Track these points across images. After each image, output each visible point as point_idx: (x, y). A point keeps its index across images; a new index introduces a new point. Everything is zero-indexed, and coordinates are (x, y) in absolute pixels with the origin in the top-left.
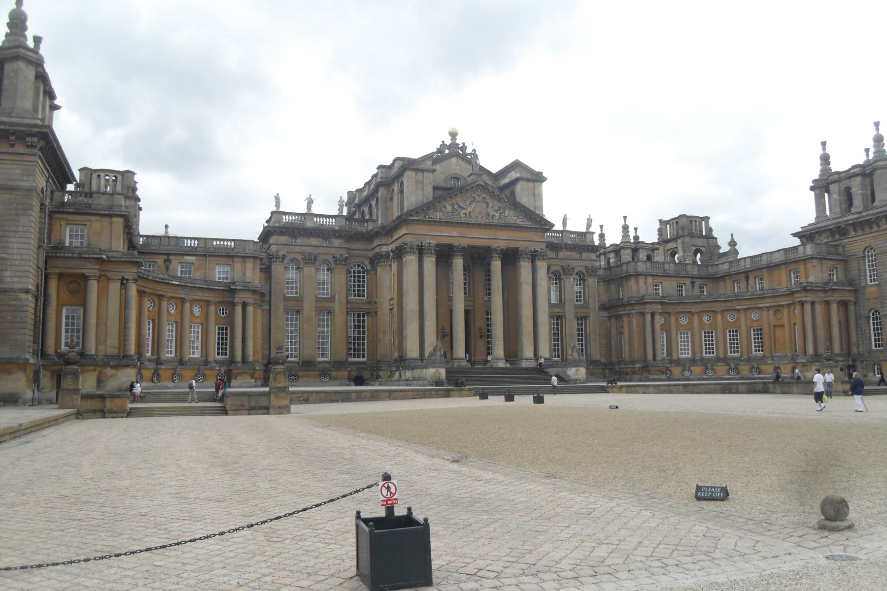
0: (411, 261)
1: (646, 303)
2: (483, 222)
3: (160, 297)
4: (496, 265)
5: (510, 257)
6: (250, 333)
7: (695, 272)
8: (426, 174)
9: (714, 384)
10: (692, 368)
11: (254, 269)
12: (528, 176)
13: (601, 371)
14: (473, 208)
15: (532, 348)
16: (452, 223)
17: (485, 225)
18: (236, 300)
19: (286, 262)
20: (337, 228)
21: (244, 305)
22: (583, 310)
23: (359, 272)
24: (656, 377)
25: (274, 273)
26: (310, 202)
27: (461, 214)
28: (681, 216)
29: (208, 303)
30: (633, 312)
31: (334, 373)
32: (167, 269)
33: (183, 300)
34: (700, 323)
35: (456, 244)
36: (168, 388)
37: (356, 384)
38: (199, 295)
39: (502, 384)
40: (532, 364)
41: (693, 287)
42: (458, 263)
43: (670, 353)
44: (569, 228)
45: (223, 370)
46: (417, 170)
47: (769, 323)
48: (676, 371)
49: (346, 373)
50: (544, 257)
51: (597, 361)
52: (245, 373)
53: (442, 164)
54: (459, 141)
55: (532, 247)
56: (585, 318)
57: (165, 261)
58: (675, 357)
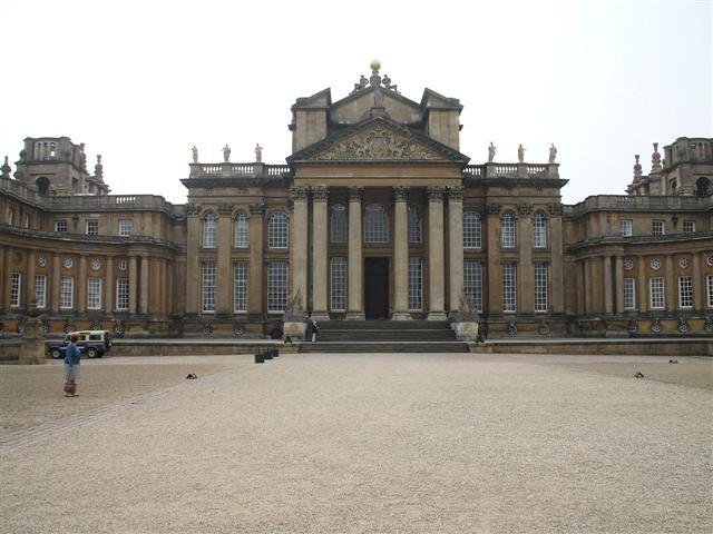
2: (384, 159)
4: (401, 207)
5: (419, 198)
6: (144, 286)
8: (318, 113)
9: (630, 343)
10: (662, 322)
11: (154, 222)
12: (441, 105)
14: (374, 146)
15: (442, 299)
17: (385, 163)
18: (130, 254)
20: (254, 176)
21: (139, 259)
22: (544, 255)
23: (281, 220)
25: (189, 227)
26: (227, 152)
28: (680, 139)
29: (105, 257)
30: (592, 256)
31: (248, 326)
32: (75, 226)
33: (78, 256)
35: (351, 186)
37: (273, 338)
38: (95, 250)
39: (208, 339)
40: (443, 318)
41: (675, 224)
42: (355, 206)
43: (638, 305)
44: (525, 161)
45: (119, 321)
46: (308, 110)
48: (644, 327)
49: (261, 326)
50: (457, 195)
51: (560, 314)
54: (381, 74)
55: (443, 184)
56: (546, 264)
57: (74, 219)
58: (643, 309)
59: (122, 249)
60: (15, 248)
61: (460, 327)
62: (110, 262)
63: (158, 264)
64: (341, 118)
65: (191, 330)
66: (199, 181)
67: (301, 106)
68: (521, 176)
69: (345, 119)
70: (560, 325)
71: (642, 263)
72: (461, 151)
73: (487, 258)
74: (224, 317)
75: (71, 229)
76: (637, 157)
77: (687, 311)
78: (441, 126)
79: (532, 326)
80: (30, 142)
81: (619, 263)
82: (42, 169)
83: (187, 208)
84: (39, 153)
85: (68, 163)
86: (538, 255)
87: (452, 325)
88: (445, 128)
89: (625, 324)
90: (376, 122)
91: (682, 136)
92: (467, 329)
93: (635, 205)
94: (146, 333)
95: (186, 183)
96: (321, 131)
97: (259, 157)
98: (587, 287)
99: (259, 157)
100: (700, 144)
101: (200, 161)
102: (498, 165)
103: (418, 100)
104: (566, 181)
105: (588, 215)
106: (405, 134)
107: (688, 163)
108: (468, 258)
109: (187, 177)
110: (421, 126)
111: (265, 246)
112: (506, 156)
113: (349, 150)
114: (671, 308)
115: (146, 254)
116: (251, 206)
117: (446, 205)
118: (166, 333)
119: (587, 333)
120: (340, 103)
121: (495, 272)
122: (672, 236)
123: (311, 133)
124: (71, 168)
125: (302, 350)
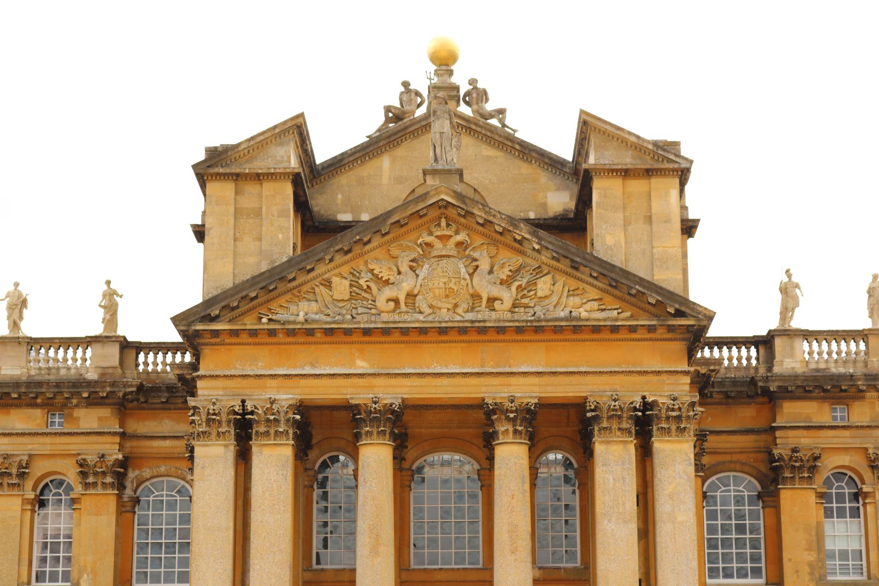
4: (511, 456)
8: (268, 187)
12: (627, 160)
14: (432, 281)
16: (348, 332)
17: (463, 331)
20: (92, 376)
27: (381, 303)
35: (359, 394)
42: (376, 458)
50: (678, 421)
53: (401, 151)
54: (461, 79)
55: (632, 394)
67: (217, 167)
72: (693, 297)
78: (627, 223)
88: (638, 227)
96: (281, 235)
97: (111, 319)
99: (111, 319)
102: (807, 335)
103: (566, 152)
110: (573, 225)
113: (357, 293)
116: (82, 464)
117: (645, 453)
120: (338, 164)
123: (248, 244)
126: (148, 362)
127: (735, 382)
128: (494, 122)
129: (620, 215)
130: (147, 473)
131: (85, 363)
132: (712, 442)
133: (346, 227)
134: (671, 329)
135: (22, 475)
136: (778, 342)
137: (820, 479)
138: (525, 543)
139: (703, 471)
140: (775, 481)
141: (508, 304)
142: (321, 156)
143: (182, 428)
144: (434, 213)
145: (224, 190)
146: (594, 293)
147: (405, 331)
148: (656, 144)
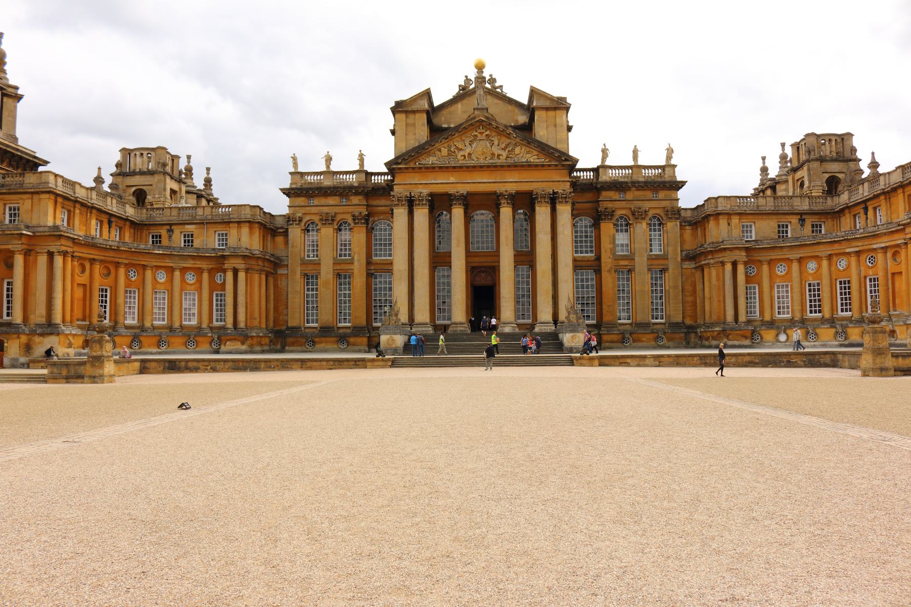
0: (401, 214)
1: (725, 249)
2: (489, 161)
3: (144, 267)
4: (506, 212)
5: (525, 202)
6: (241, 299)
7: (805, 206)
8: (418, 115)
11: (251, 233)
12: (548, 104)
13: (682, 335)
14: (477, 149)
16: (447, 167)
17: (488, 167)
18: (226, 266)
19: (303, 224)
20: (356, 184)
21: (236, 272)
24: (736, 343)
26: (329, 159)
27: (459, 157)
28: (807, 135)
31: (352, 340)
32: (170, 237)
34: (801, 273)
35: (451, 190)
36: (151, 353)
38: (189, 264)
40: (551, 328)
41: (802, 225)
42: (458, 213)
44: (641, 162)
46: (406, 112)
47: (886, 270)
49: (365, 340)
50: (565, 199)
52: (235, 339)
53: (464, 102)
54: (486, 74)
55: (549, 188)
56: (663, 271)
58: (767, 318)
59: (219, 261)
60: (102, 261)
61: (567, 339)
62: (205, 276)
63: (256, 276)
64: (443, 120)
65: (293, 344)
66: (301, 190)
67: (399, 108)
68: (635, 178)
69: (449, 123)
70: (677, 336)
71: (765, 268)
72: (571, 153)
73: (600, 266)
74: (326, 331)
75: (165, 242)
76: (764, 158)
77: (815, 320)
78: (547, 127)
79: (648, 336)
80: (126, 152)
81: (741, 269)
82: (137, 180)
83: (289, 219)
84: (135, 165)
85: (165, 173)
86: (656, 262)
87: (560, 336)
88: (552, 128)
89: (749, 334)
90: (481, 123)
91: (810, 132)
92: (573, 339)
93: (758, 206)
94: (244, 347)
95: (287, 192)
96: (422, 133)
98: (707, 295)
100: (830, 140)
101: (300, 169)
102: (611, 167)
103: (525, 100)
104: (683, 183)
105: (707, 217)
106: (508, 136)
107: (817, 160)
108: (578, 265)
109: (288, 186)
110: (527, 128)
111: (369, 255)
112: (620, 157)
114: (798, 317)
115: (243, 266)
116: (353, 216)
117: (554, 210)
118: (266, 348)
119: (707, 343)
120: (443, 106)
121: (608, 280)
122: (797, 239)
124: (168, 179)
125: (394, 364)
126: (375, 179)
127: (585, 184)
128: (498, 90)
129: (545, 124)
130: (376, 219)
131: (352, 179)
132: (577, 205)
133: (446, 129)
134: (563, 165)
135: (333, 220)
136: (601, 170)
137: (614, 219)
138: (511, 242)
139: (574, 216)
140: (599, 220)
141: (505, 157)
142: (437, 102)
143: (388, 203)
144: (478, 124)
145: (402, 117)
146: (535, 153)
147: (468, 167)
148: (558, 98)
